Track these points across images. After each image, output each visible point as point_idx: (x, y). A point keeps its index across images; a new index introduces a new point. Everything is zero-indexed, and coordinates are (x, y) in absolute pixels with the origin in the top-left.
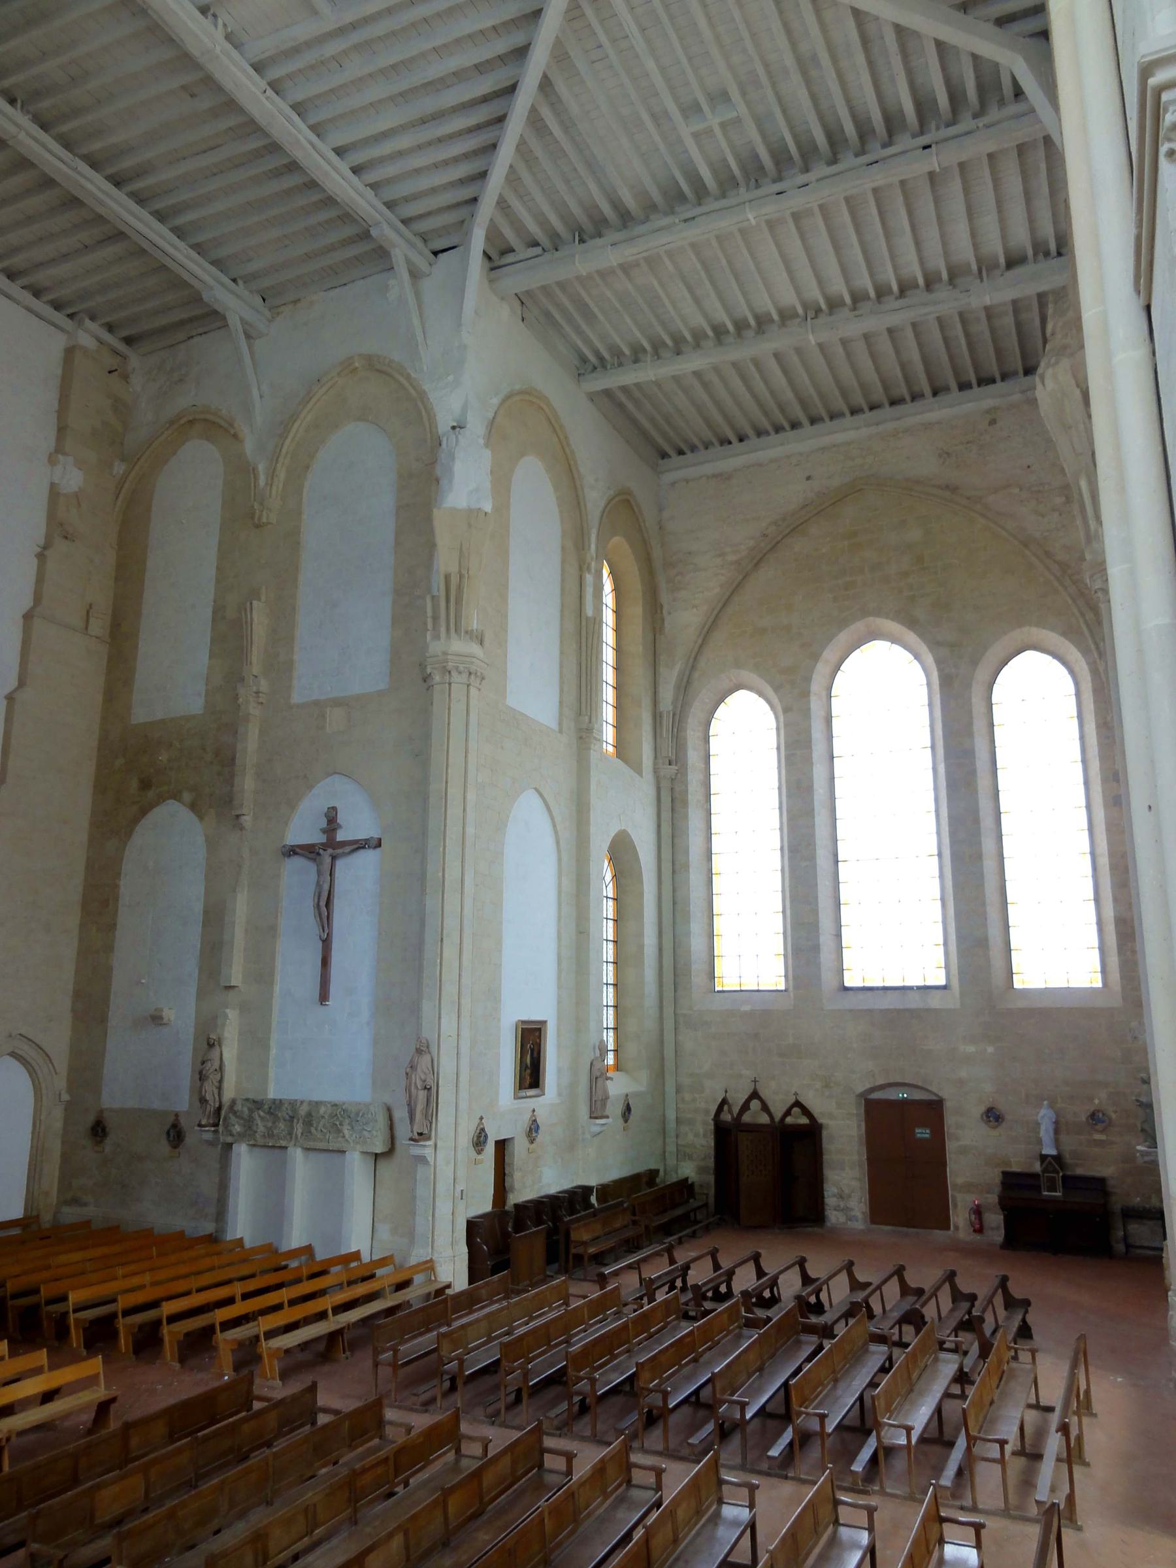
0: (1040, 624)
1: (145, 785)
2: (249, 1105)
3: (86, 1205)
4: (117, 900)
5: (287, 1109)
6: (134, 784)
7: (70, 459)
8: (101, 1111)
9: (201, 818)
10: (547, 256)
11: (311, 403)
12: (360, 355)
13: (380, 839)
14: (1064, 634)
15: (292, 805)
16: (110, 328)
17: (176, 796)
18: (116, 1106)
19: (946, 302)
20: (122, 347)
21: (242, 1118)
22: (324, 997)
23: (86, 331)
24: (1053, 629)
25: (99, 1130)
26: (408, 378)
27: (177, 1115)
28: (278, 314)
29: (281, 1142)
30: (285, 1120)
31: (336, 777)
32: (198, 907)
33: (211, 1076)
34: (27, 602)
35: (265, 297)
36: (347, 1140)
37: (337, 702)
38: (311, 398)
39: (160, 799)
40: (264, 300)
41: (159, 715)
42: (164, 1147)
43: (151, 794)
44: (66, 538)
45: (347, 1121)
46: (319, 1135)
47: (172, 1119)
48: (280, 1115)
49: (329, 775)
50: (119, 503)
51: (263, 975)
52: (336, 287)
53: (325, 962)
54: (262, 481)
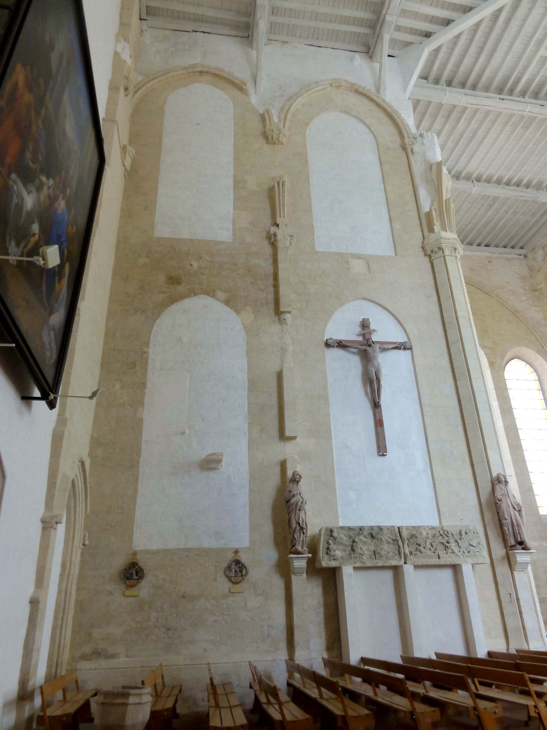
0: (527, 346)
2: (344, 532)
3: (114, 656)
4: (146, 363)
5: (387, 533)
6: (161, 279)
8: (135, 554)
9: (238, 312)
10: (427, 85)
11: (310, 92)
12: (346, 81)
14: (538, 352)
15: (329, 314)
17: (210, 292)
18: (154, 546)
19: (530, 194)
21: (342, 544)
22: (382, 450)
24: (532, 349)
26: (384, 101)
27: (236, 552)
28: (270, 44)
29: (390, 561)
30: (388, 543)
31: (363, 302)
32: (242, 377)
36: (457, 555)
37: (359, 257)
38: (310, 90)
41: (186, 235)
42: (224, 585)
45: (452, 540)
46: (429, 553)
47: (230, 556)
48: (383, 539)
50: (135, 99)
52: (314, 46)
53: (379, 423)
54: (276, 119)
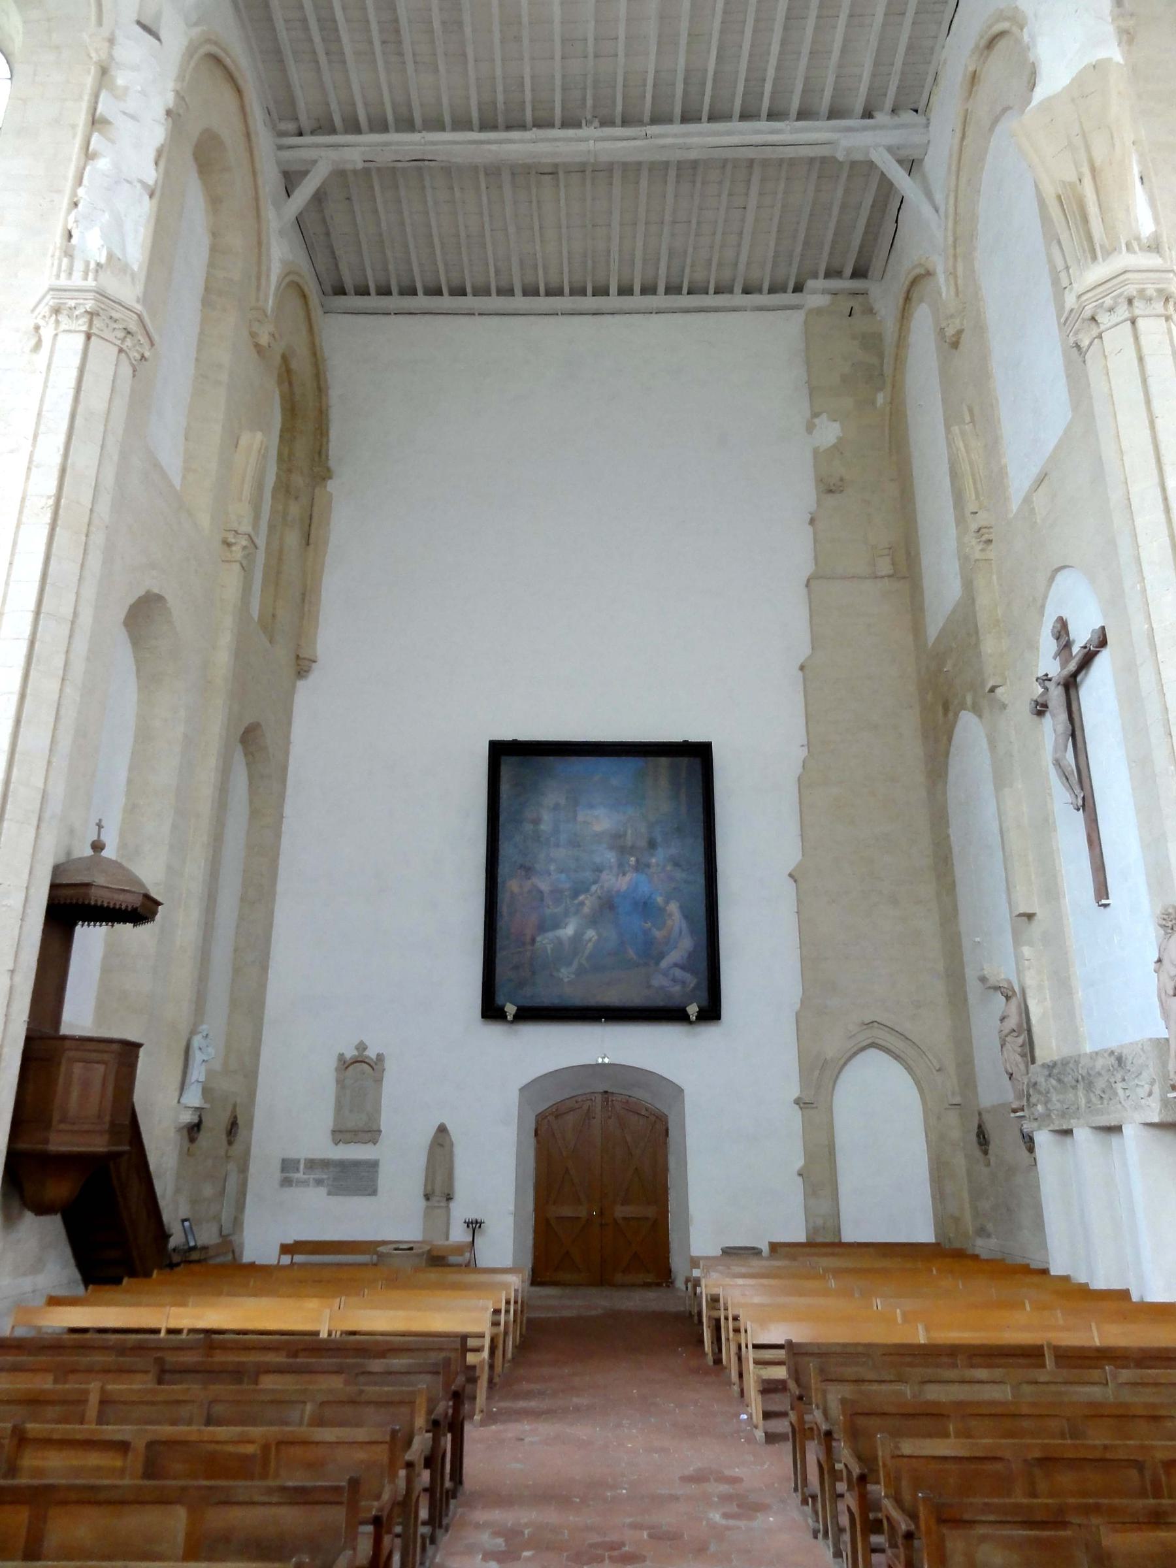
1: (946, 708)
3: (989, 1236)
7: (824, 416)
13: (1103, 628)
16: (832, 273)
20: (857, 284)
23: (814, 292)
25: (983, 1138)
33: (1007, 1039)
34: (808, 569)
35: (913, 106)
39: (956, 715)
40: (916, 111)
43: (951, 715)
44: (831, 491)
49: (1052, 579)
51: (1052, 892)
